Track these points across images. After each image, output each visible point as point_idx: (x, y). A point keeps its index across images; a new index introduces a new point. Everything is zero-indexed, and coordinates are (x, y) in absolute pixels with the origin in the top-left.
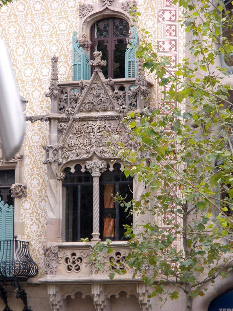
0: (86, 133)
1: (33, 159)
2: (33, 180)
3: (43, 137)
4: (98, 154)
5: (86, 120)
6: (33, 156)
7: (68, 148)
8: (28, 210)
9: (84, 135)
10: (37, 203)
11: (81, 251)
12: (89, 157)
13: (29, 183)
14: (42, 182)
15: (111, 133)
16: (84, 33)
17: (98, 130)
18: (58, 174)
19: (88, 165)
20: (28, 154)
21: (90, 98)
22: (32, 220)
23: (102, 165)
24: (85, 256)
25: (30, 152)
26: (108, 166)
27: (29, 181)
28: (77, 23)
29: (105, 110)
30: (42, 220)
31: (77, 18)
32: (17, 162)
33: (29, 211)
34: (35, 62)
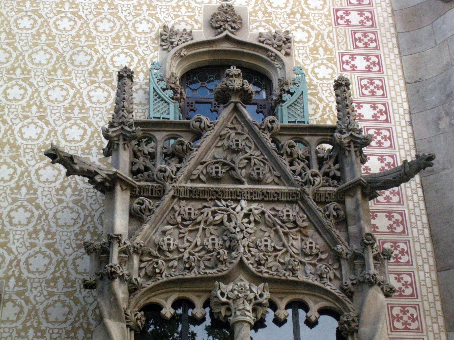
0: (211, 224)
1: (26, 309)
3: (59, 263)
4: (250, 266)
5: (209, 198)
6: (27, 301)
7: (158, 255)
9: (204, 229)
12: (224, 273)
15: (278, 227)
18: (129, 312)
20: (14, 297)
21: (220, 154)
23: (261, 295)
25: (19, 294)
26: (273, 306)
28: (154, 57)
29: (259, 181)
31: (157, 50)
34: (49, 114)
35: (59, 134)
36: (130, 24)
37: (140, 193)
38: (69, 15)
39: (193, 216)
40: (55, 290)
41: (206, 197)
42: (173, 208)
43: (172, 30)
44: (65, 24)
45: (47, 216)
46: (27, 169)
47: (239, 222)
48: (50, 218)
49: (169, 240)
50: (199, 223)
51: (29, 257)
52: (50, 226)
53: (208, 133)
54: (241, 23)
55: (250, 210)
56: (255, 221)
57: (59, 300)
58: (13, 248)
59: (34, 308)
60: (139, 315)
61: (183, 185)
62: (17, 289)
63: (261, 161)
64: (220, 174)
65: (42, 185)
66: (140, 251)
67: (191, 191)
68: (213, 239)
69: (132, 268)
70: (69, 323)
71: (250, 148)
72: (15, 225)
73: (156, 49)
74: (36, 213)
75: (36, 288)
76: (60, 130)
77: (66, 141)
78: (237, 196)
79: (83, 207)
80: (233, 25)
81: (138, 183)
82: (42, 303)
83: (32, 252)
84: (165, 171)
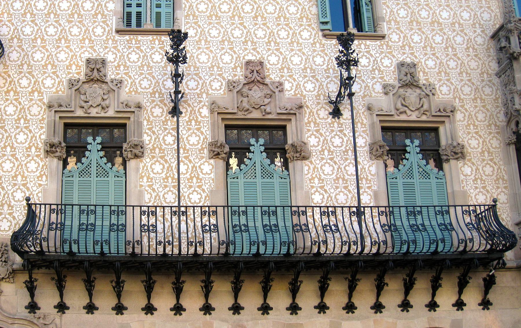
1: (467, 114)
6: (466, 110)
20: (460, 108)
32: (449, 116)
58: (453, 82)
79: (480, 59)
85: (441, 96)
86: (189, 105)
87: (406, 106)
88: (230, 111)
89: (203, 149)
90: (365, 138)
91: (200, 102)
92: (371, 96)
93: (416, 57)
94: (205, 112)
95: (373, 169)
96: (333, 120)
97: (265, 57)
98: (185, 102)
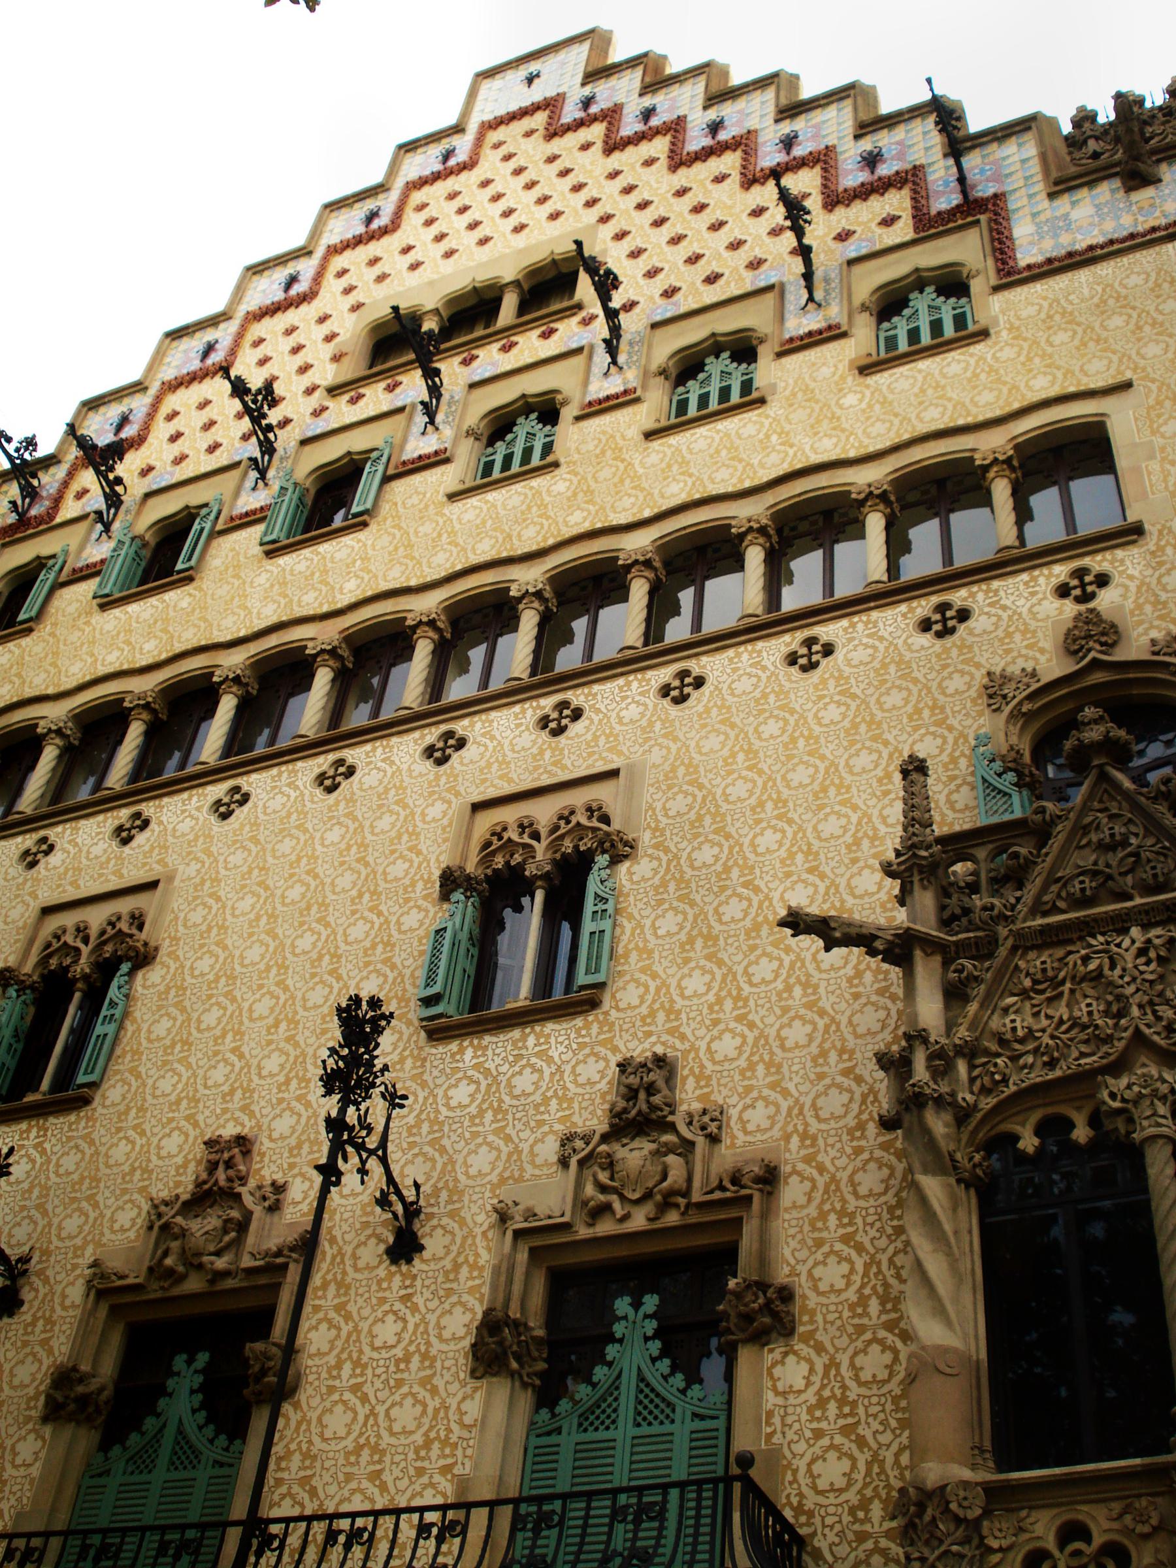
0: (1083, 979)
1: (821, 1181)
2: (824, 1263)
3: (864, 1097)
4: (1156, 1038)
5: (1075, 936)
6: (821, 1169)
8: (800, 1392)
9: (1072, 991)
10: (844, 1359)
11: (1117, 1507)
12: (1112, 1058)
13: (803, 1278)
14: (867, 1266)
16: (1014, 740)
17: (1138, 956)
18: (958, 1156)
19: (1113, 1096)
22: (818, 1434)
24: (1146, 1529)
25: (807, 1160)
27: (803, 1269)
28: (980, 727)
30: (868, 1434)
33: (803, 1397)
35: (842, 889)
36: (934, 685)
37: (957, 953)
38: (836, 698)
39: (1050, 973)
40: (863, 1143)
41: (1070, 936)
42: (1017, 967)
43: (1003, 676)
44: (833, 713)
45: (838, 1025)
46: (798, 955)
47: (1130, 965)
48: (843, 1027)
49: (1013, 1021)
50: (1063, 982)
51: (817, 1096)
52: (843, 1040)
53: (1059, 828)
54: (1116, 632)
55: (1149, 941)
56: (1159, 957)
57: (871, 1159)
58: (791, 1086)
59: (833, 1178)
60: (977, 1157)
61: (1028, 924)
62: (803, 1152)
63: (1157, 853)
64: (1088, 893)
65: (825, 976)
66: (966, 1051)
67: (1044, 930)
68: (1089, 1005)
69: (957, 1081)
70: (891, 1192)
71: (1136, 835)
72: (790, 1050)
73: (980, 714)
74: (821, 1023)
75: (833, 1146)
76: (842, 882)
77: (855, 897)
78: (1124, 921)
80: (1103, 639)
81: (954, 938)
82: (844, 1169)
83: (820, 1088)
84: (992, 908)
85: (741, 1138)
86: (46, 1281)
87: (615, 1191)
88: (130, 1281)
89: (36, 1398)
90: (472, 1310)
91: (75, 1267)
92: (520, 1179)
93: (683, 1037)
94: (76, 1293)
95: (473, 1409)
96: (393, 1268)
97: (265, 1121)
98: (40, 1273)
